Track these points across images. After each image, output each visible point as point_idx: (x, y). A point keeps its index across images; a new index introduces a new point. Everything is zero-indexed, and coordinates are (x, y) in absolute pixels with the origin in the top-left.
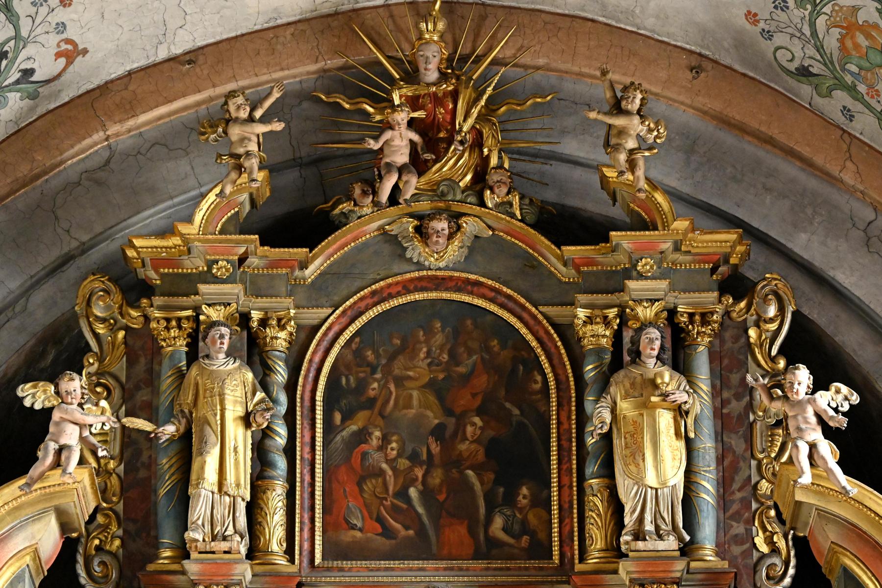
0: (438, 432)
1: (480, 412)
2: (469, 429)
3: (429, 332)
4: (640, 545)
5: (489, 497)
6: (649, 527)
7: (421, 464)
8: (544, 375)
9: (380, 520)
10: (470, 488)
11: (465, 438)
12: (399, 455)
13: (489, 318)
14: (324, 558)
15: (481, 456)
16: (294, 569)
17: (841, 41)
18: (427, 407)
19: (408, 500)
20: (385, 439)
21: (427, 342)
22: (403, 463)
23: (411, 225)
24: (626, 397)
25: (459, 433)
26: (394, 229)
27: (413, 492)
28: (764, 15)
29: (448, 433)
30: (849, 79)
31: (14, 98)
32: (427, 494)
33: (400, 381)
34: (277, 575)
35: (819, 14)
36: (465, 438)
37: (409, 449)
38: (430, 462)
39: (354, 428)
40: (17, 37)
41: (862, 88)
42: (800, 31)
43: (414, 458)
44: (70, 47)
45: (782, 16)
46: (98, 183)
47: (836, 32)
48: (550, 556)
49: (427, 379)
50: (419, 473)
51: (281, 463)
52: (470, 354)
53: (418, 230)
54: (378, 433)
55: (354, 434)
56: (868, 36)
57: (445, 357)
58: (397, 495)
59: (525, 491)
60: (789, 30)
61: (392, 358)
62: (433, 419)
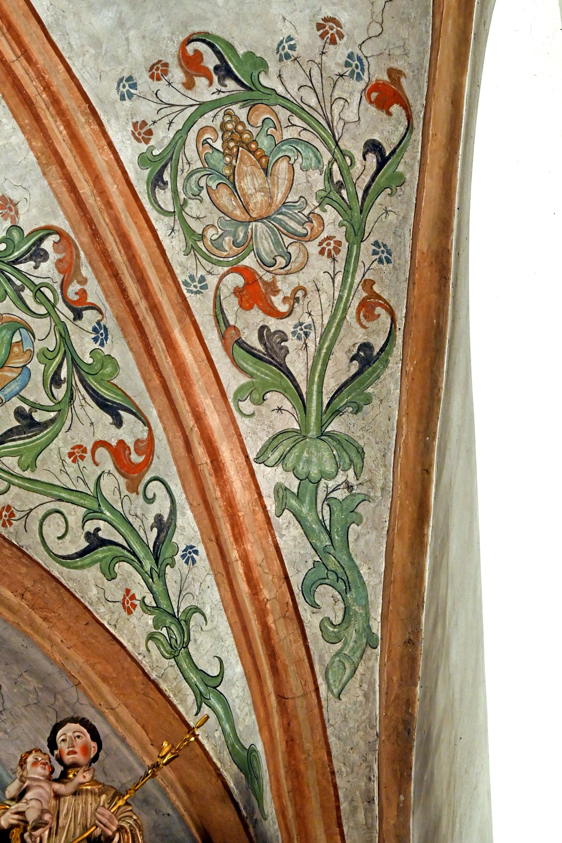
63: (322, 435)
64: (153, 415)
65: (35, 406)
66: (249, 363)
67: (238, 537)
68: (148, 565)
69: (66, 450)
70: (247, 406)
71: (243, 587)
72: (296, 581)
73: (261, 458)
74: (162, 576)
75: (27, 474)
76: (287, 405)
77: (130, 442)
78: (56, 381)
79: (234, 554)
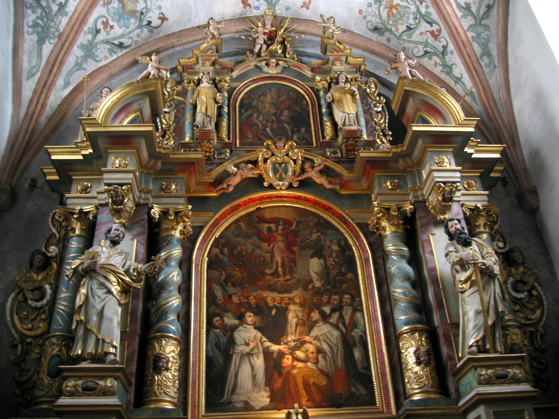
0: (275, 114)
1: (287, 109)
2: (284, 114)
3: (271, 91)
4: (346, 128)
5: (292, 131)
6: (347, 123)
7: (270, 122)
8: (307, 101)
9: (257, 136)
10: (286, 128)
11: (283, 116)
12: (263, 120)
13: (288, 88)
14: (240, 145)
15: (289, 120)
16: (230, 142)
17: (388, 13)
18: (271, 108)
19: (266, 131)
20: (258, 117)
21: (270, 93)
22: (264, 122)
23: (264, 63)
24: (336, 92)
25: (281, 114)
26: (259, 64)
27: (268, 129)
28: (364, 10)
29: (278, 115)
30: (389, 27)
31: (145, 30)
32: (272, 130)
33: (262, 102)
34: (227, 143)
35: (381, 5)
36: (283, 116)
37: (266, 118)
38: (273, 122)
39: (248, 113)
40: (146, 8)
41: (393, 29)
42: (375, 13)
43: (268, 121)
44: (162, 16)
45: (370, 9)
46: (170, 58)
47: (386, 10)
48: (312, 144)
49: (270, 102)
50: (269, 124)
51: (226, 116)
52: (283, 95)
53: (266, 64)
54: (256, 115)
55: (248, 115)
56: (397, 9)
57: (276, 97)
58: (262, 130)
59: (303, 129)
60: (372, 14)
61: (260, 96)
62: (273, 111)
63: (481, 24)
64: (441, 24)
65: (411, 25)
66: (463, 10)
67: (465, 47)
68: (441, 56)
69: (418, 33)
70: (463, 20)
71: (467, 58)
72: (478, 55)
73: (468, 30)
74: (444, 58)
75: (409, 39)
76: (472, 19)
77: (435, 30)
78: (416, 18)
79: (464, 51)
